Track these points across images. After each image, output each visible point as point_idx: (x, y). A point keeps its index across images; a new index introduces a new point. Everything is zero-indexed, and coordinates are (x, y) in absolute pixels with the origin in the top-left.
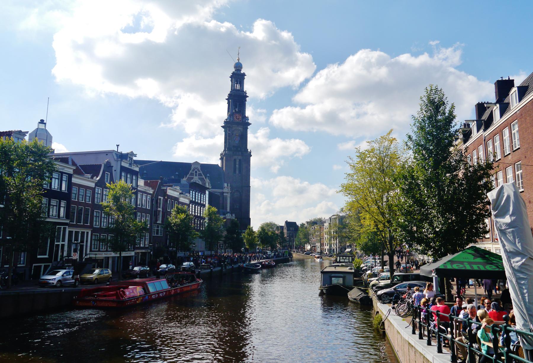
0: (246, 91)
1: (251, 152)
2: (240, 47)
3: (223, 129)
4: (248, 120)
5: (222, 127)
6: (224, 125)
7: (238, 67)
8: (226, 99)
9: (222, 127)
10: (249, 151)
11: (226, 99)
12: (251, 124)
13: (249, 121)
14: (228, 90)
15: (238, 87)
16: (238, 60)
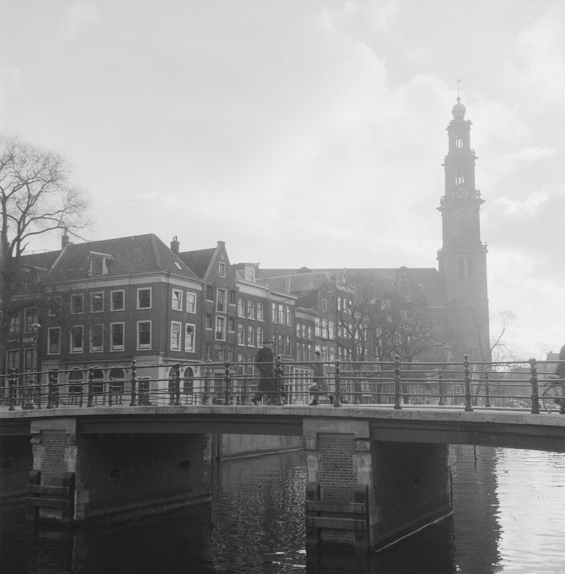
0: (474, 149)
1: (486, 246)
2: (460, 81)
3: (440, 213)
4: (479, 196)
5: (437, 209)
6: (440, 205)
7: (459, 111)
8: (442, 165)
9: (437, 209)
10: (483, 244)
11: (442, 165)
12: (484, 201)
13: (480, 197)
14: (446, 151)
15: (459, 144)
16: (459, 99)
